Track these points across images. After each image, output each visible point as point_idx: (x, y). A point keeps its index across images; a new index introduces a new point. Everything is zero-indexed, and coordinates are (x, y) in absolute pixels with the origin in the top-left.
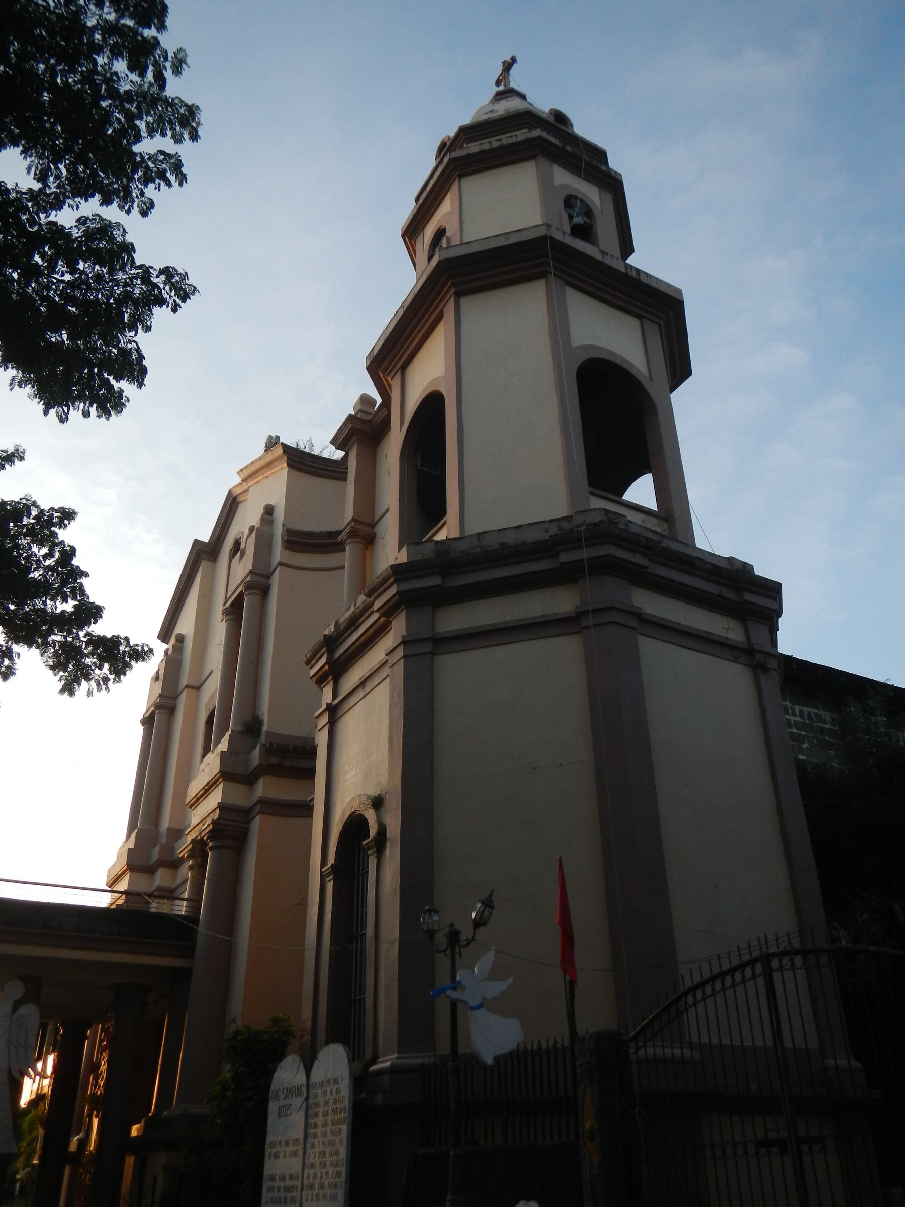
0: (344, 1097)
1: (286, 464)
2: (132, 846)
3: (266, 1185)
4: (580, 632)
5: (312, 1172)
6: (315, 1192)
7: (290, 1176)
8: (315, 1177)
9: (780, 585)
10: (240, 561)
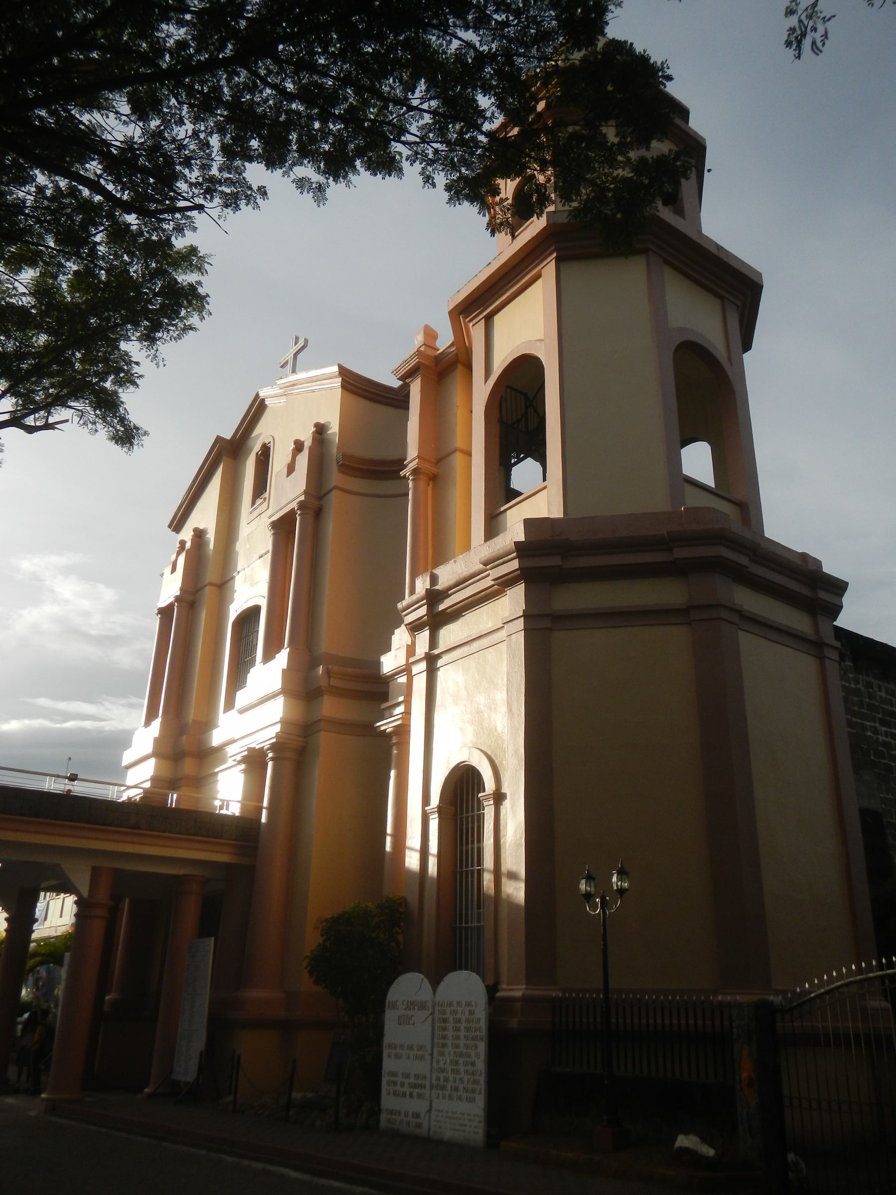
0: (479, 1020)
2: (156, 734)
3: (385, 1080)
4: (689, 624)
5: (442, 1076)
6: (447, 1093)
7: (415, 1076)
8: (446, 1080)
9: (847, 584)
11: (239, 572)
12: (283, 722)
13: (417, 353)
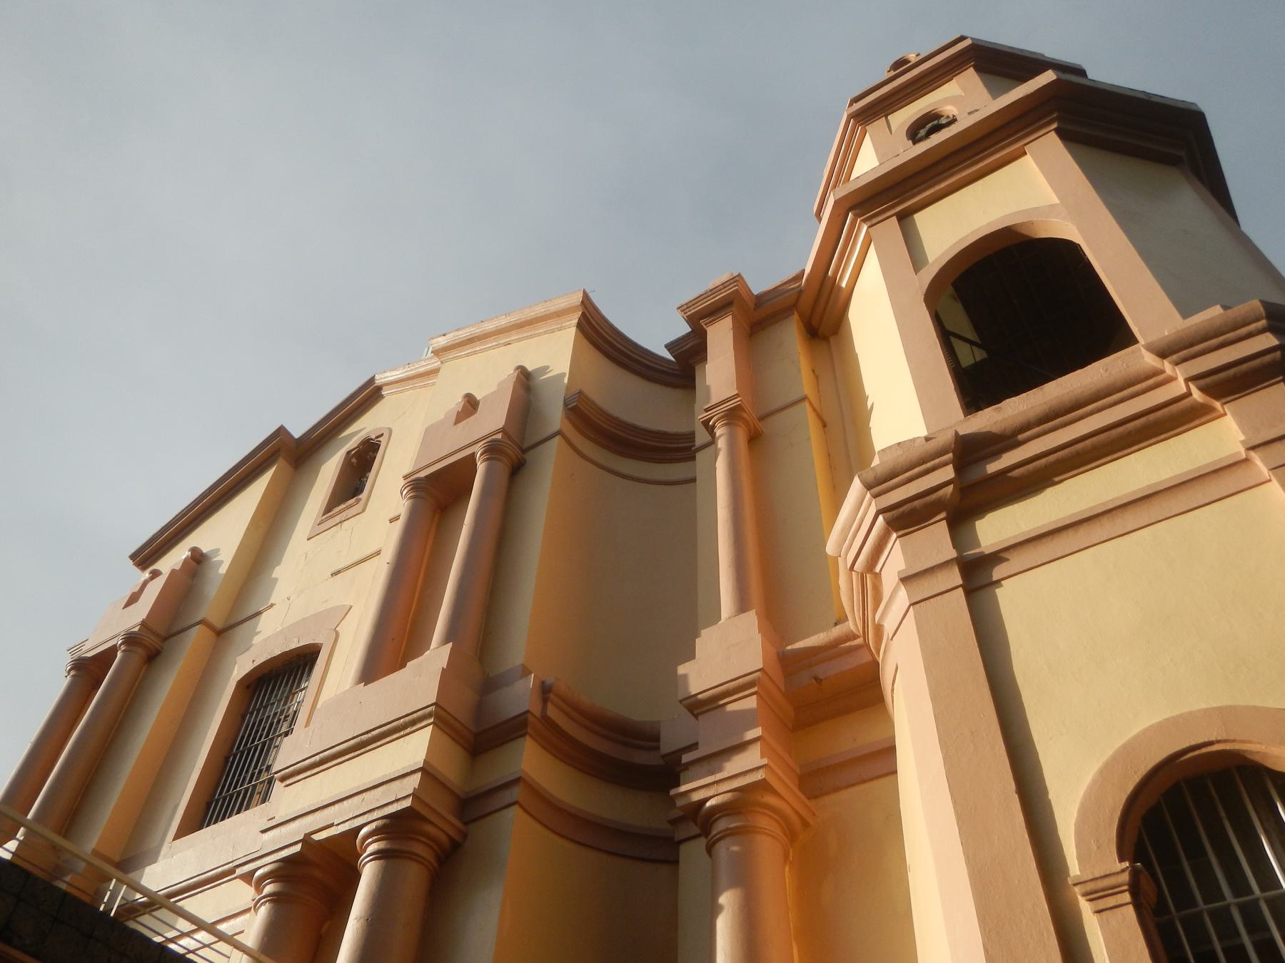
1: (575, 321)
10: (455, 424)
11: (272, 605)
12: (426, 771)
13: (737, 278)
